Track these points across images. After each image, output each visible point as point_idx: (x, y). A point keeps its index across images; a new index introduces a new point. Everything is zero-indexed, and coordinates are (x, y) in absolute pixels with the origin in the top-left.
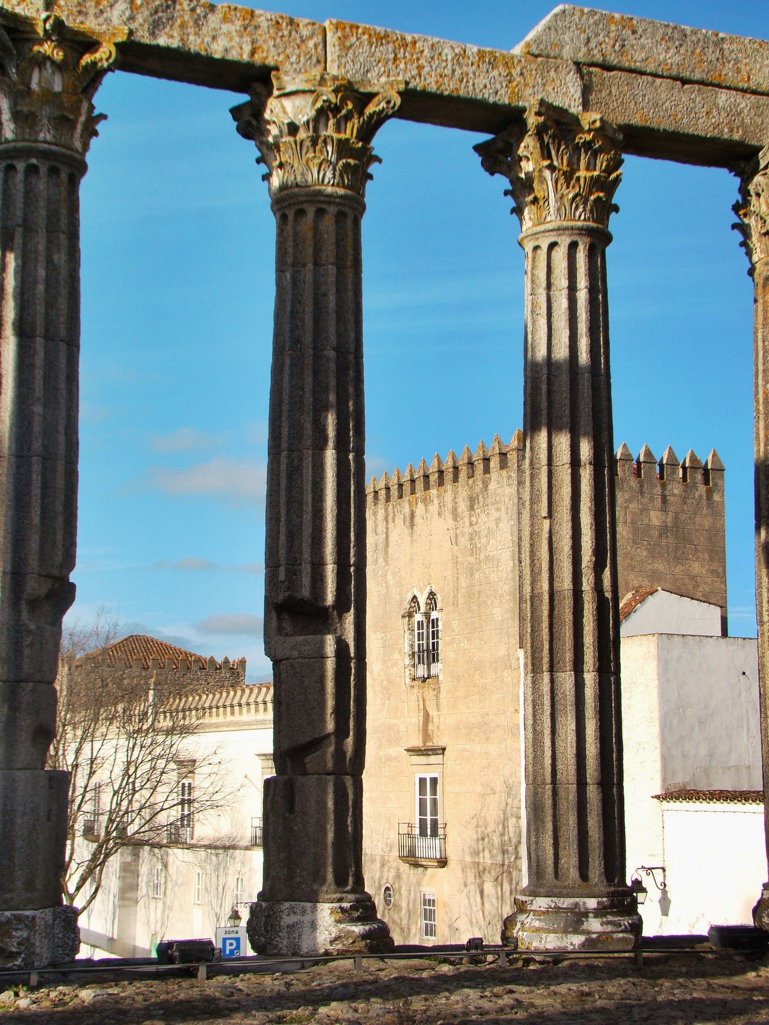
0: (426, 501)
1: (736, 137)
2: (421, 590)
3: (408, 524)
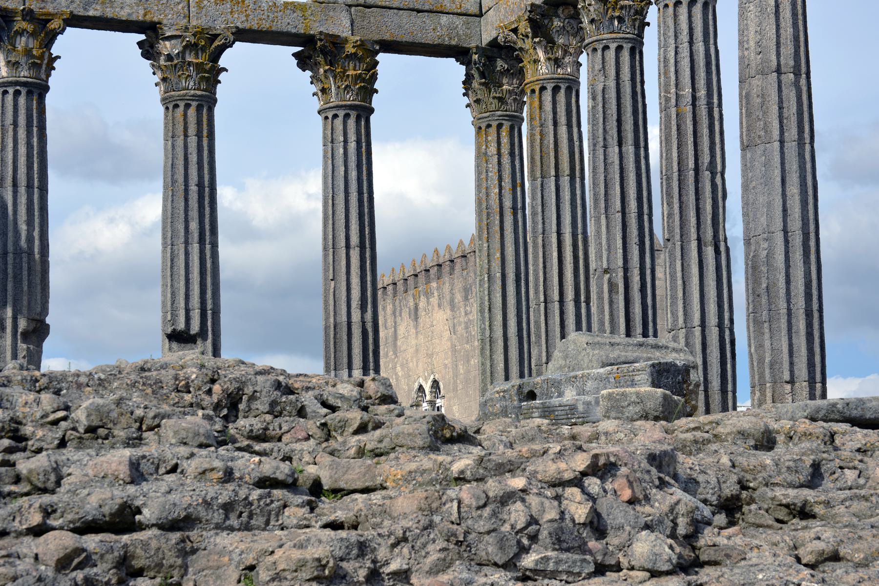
0: (428, 294)
1: (453, 43)
2: (426, 380)
3: (413, 317)
